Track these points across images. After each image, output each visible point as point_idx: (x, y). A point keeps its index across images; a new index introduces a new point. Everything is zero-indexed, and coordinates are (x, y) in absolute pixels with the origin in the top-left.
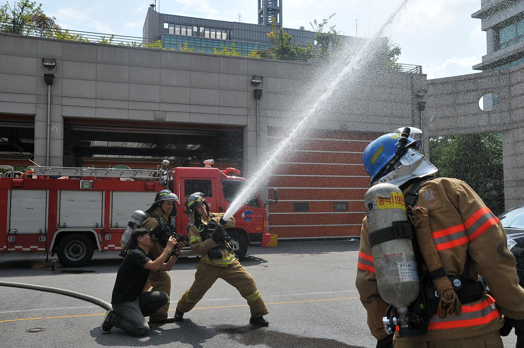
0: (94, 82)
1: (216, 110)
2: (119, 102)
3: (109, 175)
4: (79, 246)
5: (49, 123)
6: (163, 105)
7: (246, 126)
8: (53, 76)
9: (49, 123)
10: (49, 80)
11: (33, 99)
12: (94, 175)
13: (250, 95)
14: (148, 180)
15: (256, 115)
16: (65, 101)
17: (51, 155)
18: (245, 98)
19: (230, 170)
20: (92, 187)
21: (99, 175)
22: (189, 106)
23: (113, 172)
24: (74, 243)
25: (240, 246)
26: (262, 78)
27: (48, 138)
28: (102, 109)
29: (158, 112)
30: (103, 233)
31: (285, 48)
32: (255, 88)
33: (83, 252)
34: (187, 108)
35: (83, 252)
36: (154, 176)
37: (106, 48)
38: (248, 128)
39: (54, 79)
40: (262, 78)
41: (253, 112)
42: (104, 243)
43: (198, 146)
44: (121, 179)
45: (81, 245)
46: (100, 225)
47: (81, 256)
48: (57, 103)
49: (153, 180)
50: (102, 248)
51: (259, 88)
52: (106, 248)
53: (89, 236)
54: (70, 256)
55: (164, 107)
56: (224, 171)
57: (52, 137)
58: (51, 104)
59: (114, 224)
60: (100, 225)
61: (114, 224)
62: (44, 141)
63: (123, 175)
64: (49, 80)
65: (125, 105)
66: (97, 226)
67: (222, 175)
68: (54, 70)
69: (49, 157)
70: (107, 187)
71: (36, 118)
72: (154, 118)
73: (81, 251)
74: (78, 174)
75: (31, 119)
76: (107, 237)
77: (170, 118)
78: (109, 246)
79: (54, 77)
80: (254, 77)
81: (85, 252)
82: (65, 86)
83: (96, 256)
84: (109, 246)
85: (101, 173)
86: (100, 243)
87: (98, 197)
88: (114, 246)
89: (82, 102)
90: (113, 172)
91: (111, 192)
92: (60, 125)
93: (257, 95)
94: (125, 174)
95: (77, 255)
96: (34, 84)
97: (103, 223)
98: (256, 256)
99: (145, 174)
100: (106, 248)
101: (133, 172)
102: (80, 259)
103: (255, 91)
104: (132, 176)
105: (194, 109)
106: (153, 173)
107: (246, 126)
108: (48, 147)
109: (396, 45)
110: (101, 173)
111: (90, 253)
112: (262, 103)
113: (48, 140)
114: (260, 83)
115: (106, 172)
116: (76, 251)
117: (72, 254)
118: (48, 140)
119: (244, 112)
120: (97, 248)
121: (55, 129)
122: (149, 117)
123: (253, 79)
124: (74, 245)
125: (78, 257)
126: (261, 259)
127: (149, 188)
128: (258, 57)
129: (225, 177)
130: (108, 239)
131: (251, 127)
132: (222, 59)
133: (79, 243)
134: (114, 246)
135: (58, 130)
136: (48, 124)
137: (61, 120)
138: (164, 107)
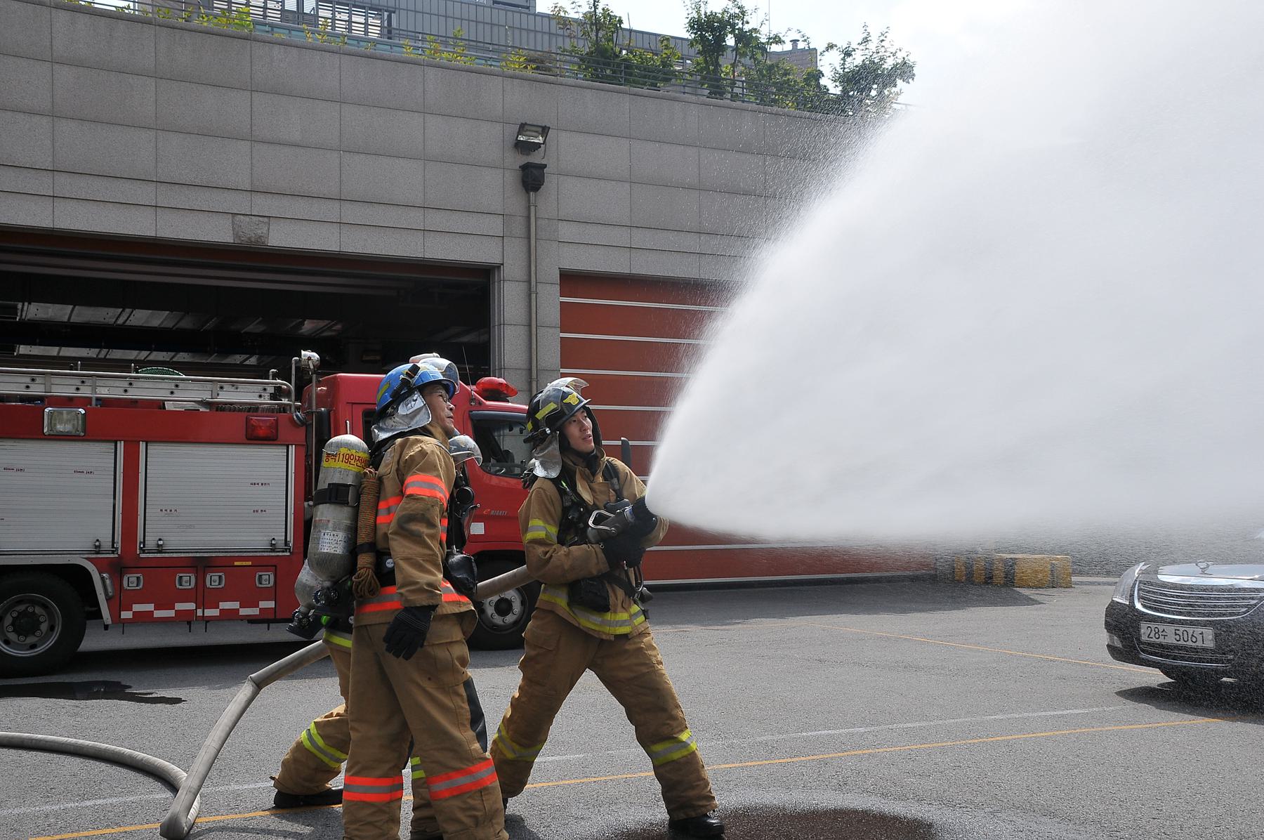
0: (45, 121)
1: (414, 218)
2: (128, 184)
3: (135, 393)
4: (38, 610)
7: (498, 267)
12: (85, 392)
13: (512, 178)
14: (253, 408)
15: (529, 238)
18: (496, 186)
19: (491, 383)
20: (84, 431)
21: (104, 392)
22: (337, 204)
23: (148, 387)
24: (20, 602)
25: (523, 603)
26: (544, 131)
29: (247, 219)
30: (117, 568)
31: (606, 50)
33: (52, 628)
34: (331, 211)
35: (52, 628)
36: (273, 397)
37: (83, 19)
40: (544, 131)
41: (518, 228)
42: (120, 600)
43: (339, 327)
44: (169, 406)
45: (45, 606)
46: (106, 545)
47: (44, 639)
49: (271, 410)
50: (116, 609)
51: (535, 158)
52: (126, 615)
53: (74, 577)
56: (474, 387)
59: (151, 543)
60: (106, 545)
61: (151, 543)
63: (179, 395)
66: (98, 549)
67: (473, 399)
70: (130, 427)
72: (236, 235)
73: (44, 627)
74: (37, 390)
76: (131, 581)
77: (281, 237)
78: (137, 608)
80: (523, 128)
81: (58, 629)
83: (93, 641)
84: (137, 608)
85: (110, 388)
86: (108, 599)
87: (100, 459)
88: (150, 607)
90: (148, 387)
91: (142, 445)
93: (532, 179)
94: (185, 392)
95: (31, 640)
97: (118, 538)
99: (246, 393)
100: (126, 615)
101: (209, 386)
102: (40, 650)
103: (525, 168)
104: (206, 396)
105: (352, 213)
106: (271, 390)
107: (498, 267)
109: (900, 55)
110: (110, 388)
111: (74, 633)
112: (546, 200)
114: (538, 146)
115: (126, 385)
116: (26, 626)
119: (495, 226)
120: (98, 615)
122: (218, 232)
123: (519, 133)
124: (22, 608)
125: (33, 646)
127: (261, 433)
128: (529, 73)
129: (480, 403)
130: (133, 586)
131: (513, 269)
132: (431, 72)
133: (33, 602)
134: (150, 607)
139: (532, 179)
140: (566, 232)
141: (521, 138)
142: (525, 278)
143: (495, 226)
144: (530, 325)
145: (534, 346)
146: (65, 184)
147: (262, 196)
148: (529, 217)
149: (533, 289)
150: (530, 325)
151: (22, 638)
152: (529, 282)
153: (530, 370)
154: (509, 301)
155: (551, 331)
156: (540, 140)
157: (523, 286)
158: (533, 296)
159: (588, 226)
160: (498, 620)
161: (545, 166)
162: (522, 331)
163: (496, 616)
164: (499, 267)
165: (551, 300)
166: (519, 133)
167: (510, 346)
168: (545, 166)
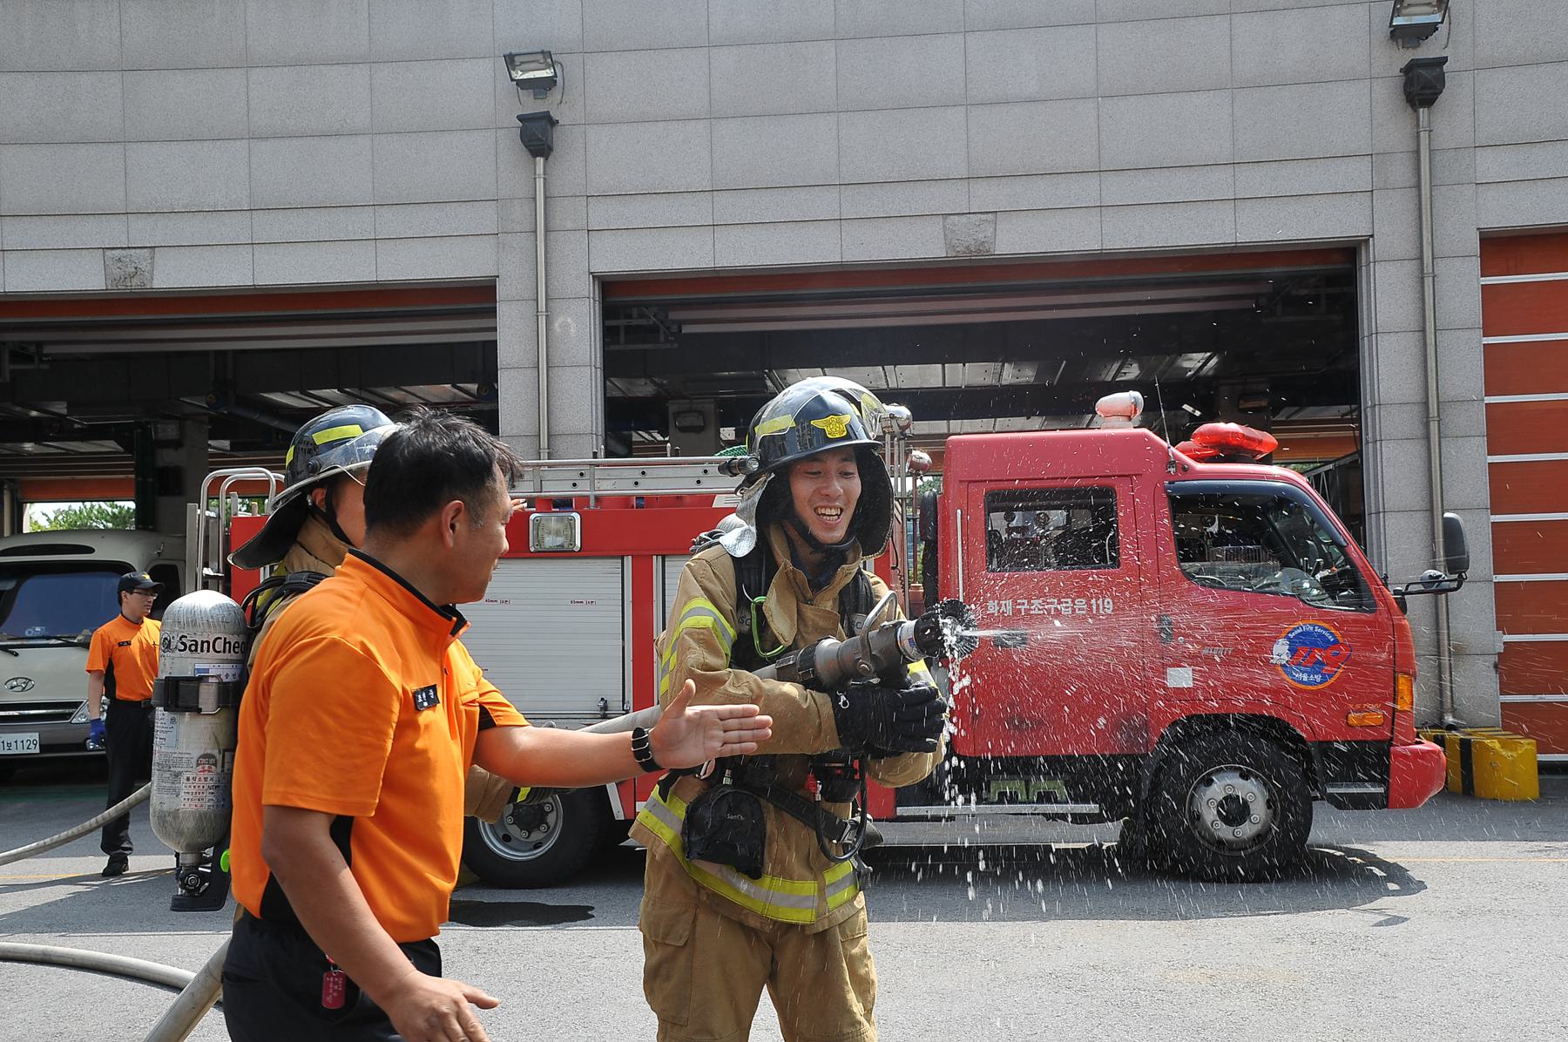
1: (1219, 183)
5: (542, 306)
6: (980, 188)
7: (1365, 241)
8: (548, 121)
9: (542, 306)
10: (538, 137)
11: (487, 218)
13: (1388, 91)
15: (1418, 186)
16: (600, 214)
17: (557, 429)
22: (1095, 178)
27: (547, 365)
28: (737, 230)
29: (964, 219)
32: (1405, 56)
34: (1085, 191)
38: (1378, 248)
39: (557, 132)
41: (1400, 171)
48: (569, 225)
51: (1429, 50)
54: (506, 839)
55: (987, 196)
57: (555, 361)
58: (547, 231)
62: (531, 373)
64: (538, 137)
65: (824, 204)
68: (556, 94)
69: (549, 436)
71: (501, 292)
72: (949, 245)
73: (551, 818)
75: (478, 297)
77: (1015, 239)
79: (553, 123)
81: (560, 824)
82: (595, 152)
89: (659, 213)
92: (586, 310)
93: (1422, 87)
95: (536, 836)
96: (489, 154)
98: (1388, 851)
103: (1410, 69)
105: (1117, 189)
107: (1365, 241)
108: (546, 400)
112: (1452, 117)
113: (551, 375)
114: (1434, 27)
117: (514, 830)
118: (551, 375)
119: (1357, 174)
121: (565, 326)
123: (1396, 12)
125: (537, 846)
126: (1395, 873)
135: (580, 329)
136: (545, 308)
137: (587, 288)
138: (987, 196)
139: (1422, 87)
140: (1490, 165)
141: (1398, 21)
142: (1414, 253)
143: (1357, 174)
144: (1425, 331)
145: (1431, 364)
146: (728, 209)
147: (984, 183)
148: (1418, 152)
149: (1428, 269)
150: (1423, 331)
151: (525, 834)
152: (1421, 258)
153: (1426, 404)
154: (1385, 299)
155: (1465, 335)
156: (1437, 18)
157: (1411, 267)
158: (1428, 281)
159: (1536, 149)
160: (1224, 832)
161: (1445, 60)
162: (1410, 342)
163: (1220, 824)
164: (1367, 241)
165: (1464, 285)
166: (1396, 12)
167: (1388, 367)
168: (1445, 60)
